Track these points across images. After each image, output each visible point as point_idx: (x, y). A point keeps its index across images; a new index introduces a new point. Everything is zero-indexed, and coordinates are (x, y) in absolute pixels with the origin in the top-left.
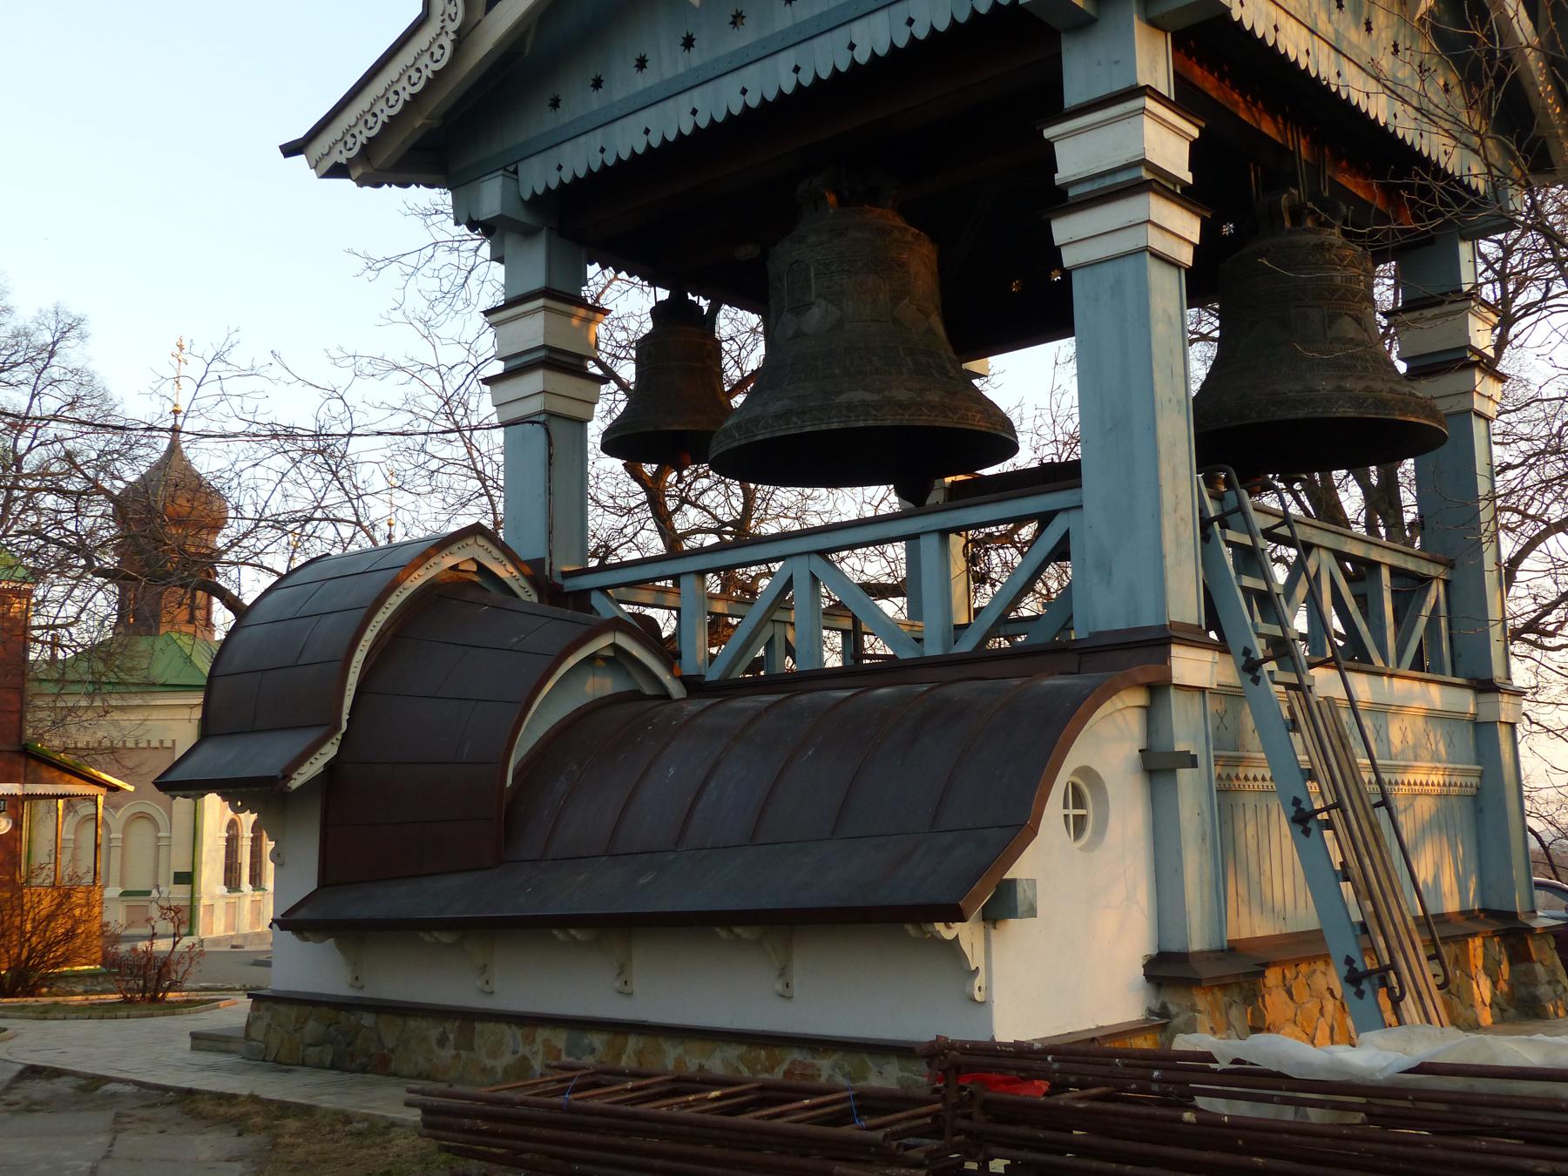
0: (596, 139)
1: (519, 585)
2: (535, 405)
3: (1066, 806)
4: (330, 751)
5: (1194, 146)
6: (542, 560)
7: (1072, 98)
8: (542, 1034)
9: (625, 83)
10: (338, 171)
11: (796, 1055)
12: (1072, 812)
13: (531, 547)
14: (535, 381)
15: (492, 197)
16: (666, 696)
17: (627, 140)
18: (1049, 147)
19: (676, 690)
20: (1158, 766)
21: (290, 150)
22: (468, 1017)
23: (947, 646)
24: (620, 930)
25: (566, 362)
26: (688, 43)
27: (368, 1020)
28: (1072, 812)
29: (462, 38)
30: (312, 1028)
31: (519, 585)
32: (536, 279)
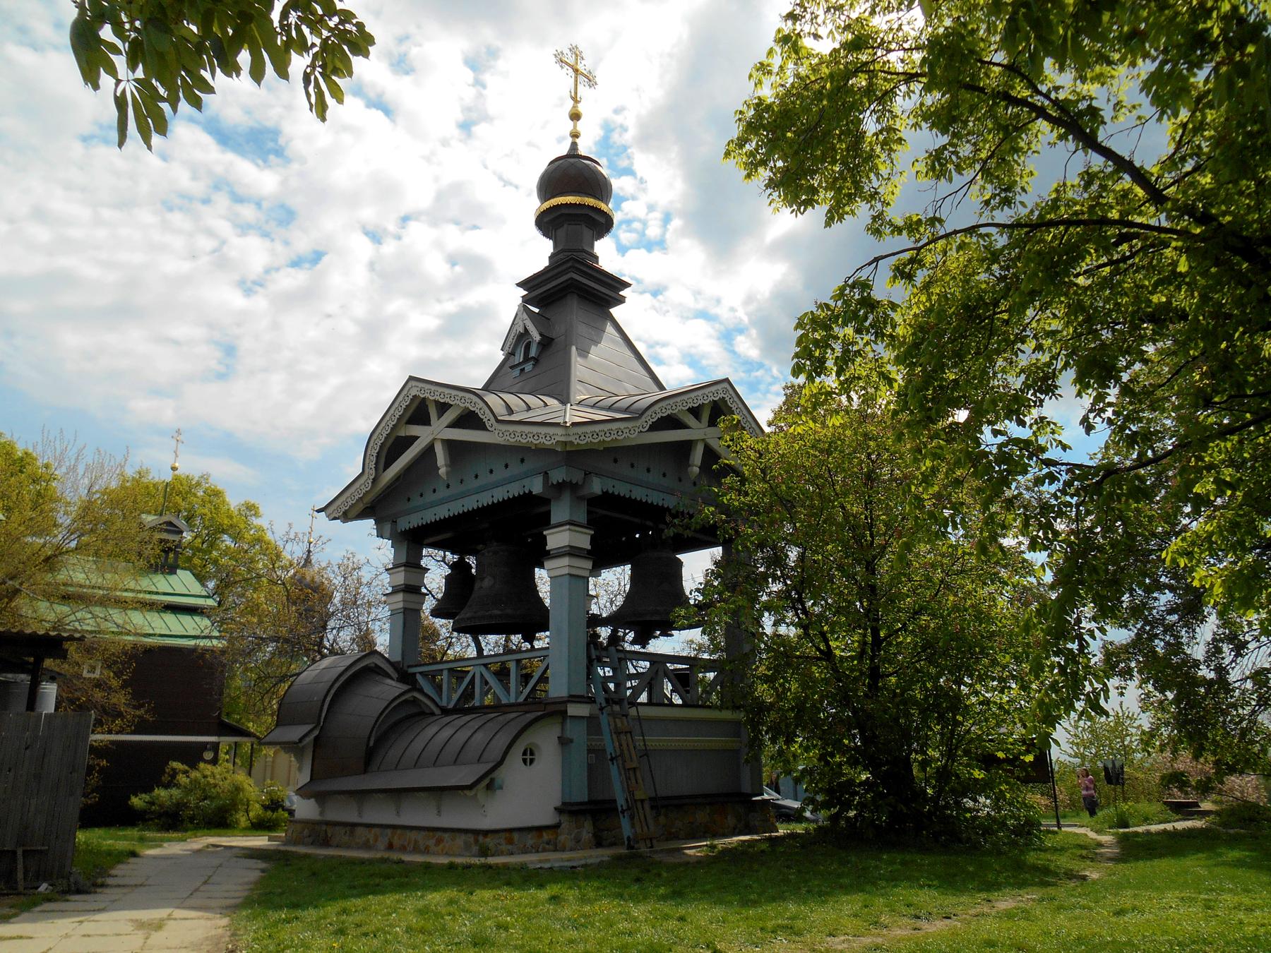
0: (420, 515)
1: (390, 670)
2: (401, 605)
3: (525, 753)
4: (316, 733)
5: (592, 537)
6: (398, 663)
7: (553, 521)
8: (374, 830)
9: (430, 497)
10: (335, 518)
11: (439, 834)
12: (528, 757)
13: (397, 658)
14: (400, 597)
15: (387, 528)
16: (433, 714)
17: (430, 516)
18: (545, 537)
19: (437, 711)
20: (564, 742)
21: (318, 511)
22: (354, 825)
23: (517, 698)
24: (398, 794)
25: (412, 590)
26: (448, 486)
27: (324, 827)
28: (528, 757)
29: (374, 481)
30: (306, 832)
31: (390, 670)
32: (403, 560)
